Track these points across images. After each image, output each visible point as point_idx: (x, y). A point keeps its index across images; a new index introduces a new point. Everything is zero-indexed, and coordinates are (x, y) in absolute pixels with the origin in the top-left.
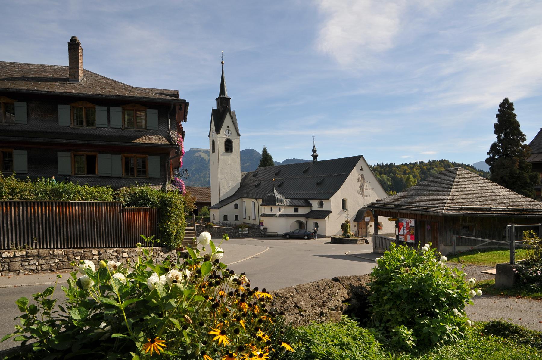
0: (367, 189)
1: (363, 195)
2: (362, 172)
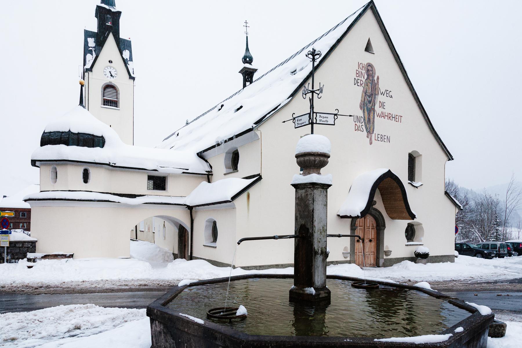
0: (383, 115)
1: (370, 131)
2: (367, 58)
